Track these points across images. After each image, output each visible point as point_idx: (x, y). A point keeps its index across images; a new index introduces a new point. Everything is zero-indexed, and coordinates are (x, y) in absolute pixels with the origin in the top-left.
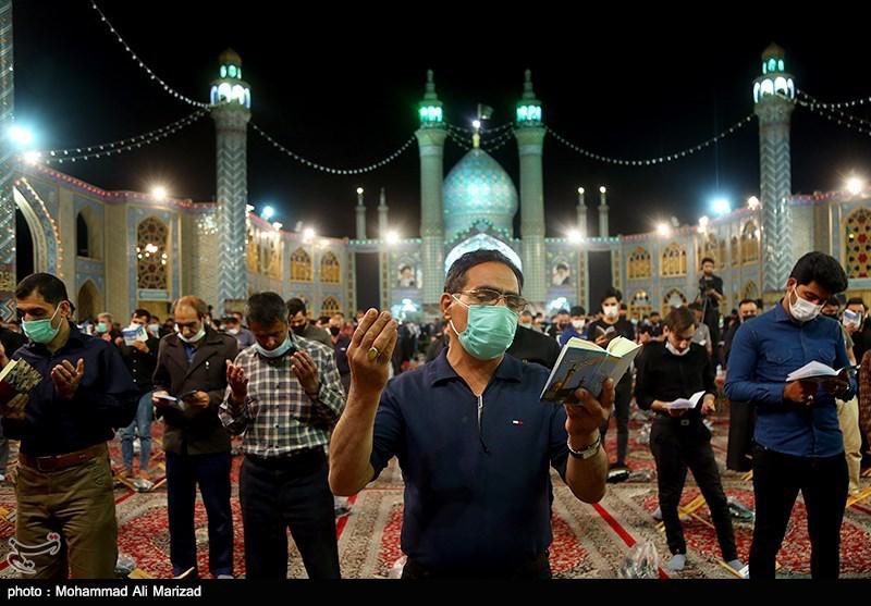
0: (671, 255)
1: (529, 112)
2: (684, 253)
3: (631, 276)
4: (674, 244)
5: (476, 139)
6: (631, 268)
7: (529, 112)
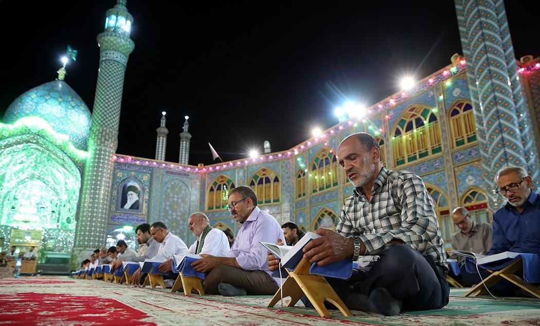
0: (261, 182)
2: (276, 180)
3: (210, 208)
4: (264, 170)
5: (62, 73)
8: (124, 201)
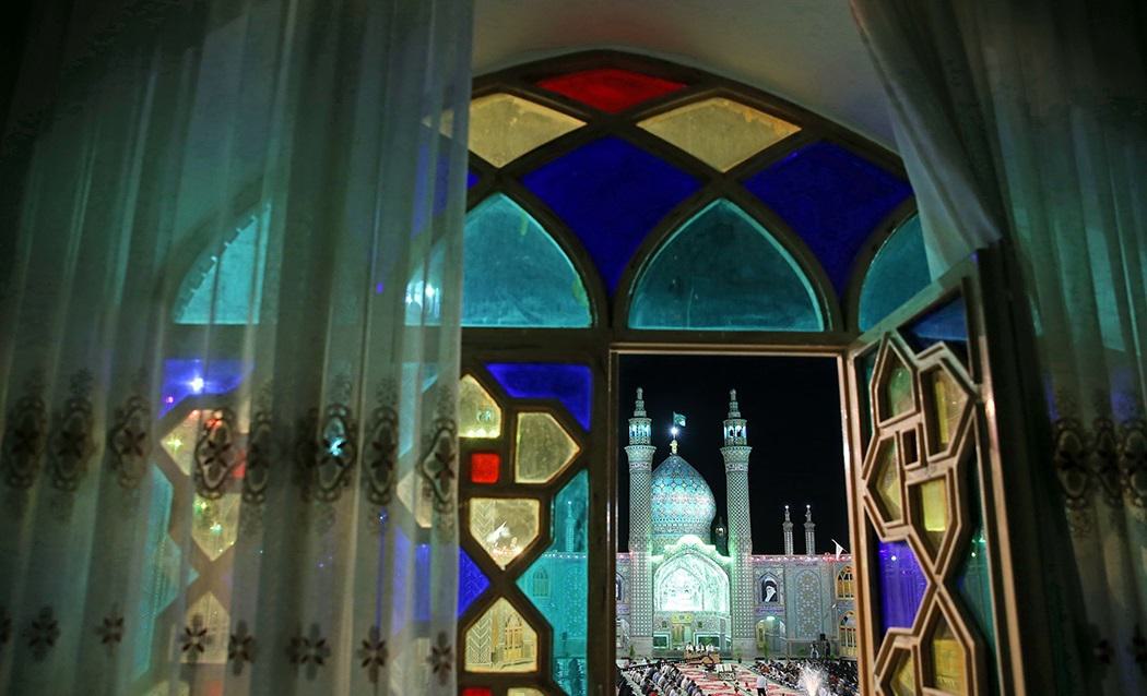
1: (736, 428)
5: (674, 445)
6: (840, 589)
7: (736, 428)
8: (765, 596)
